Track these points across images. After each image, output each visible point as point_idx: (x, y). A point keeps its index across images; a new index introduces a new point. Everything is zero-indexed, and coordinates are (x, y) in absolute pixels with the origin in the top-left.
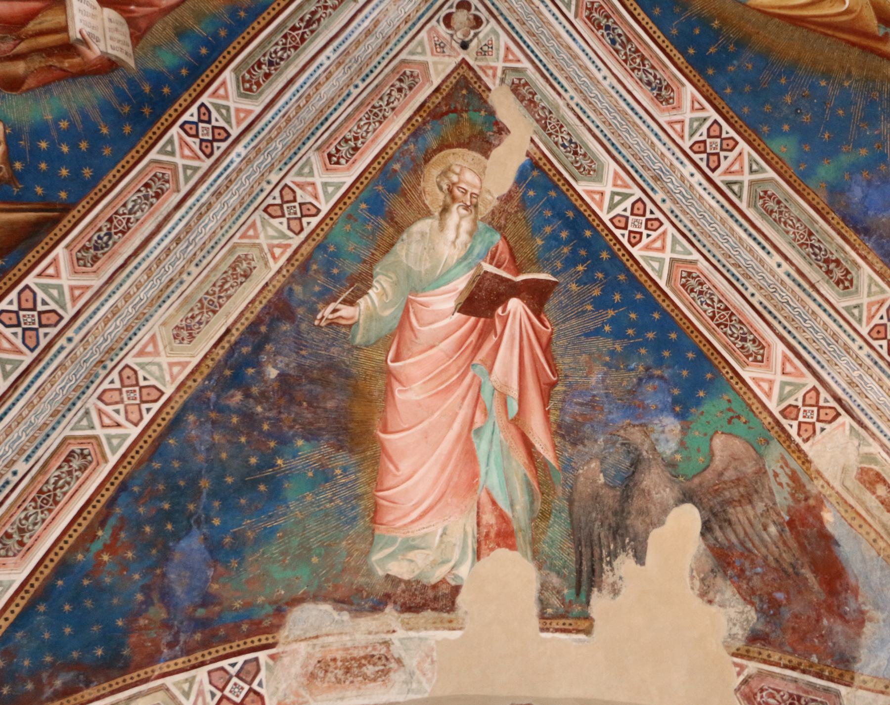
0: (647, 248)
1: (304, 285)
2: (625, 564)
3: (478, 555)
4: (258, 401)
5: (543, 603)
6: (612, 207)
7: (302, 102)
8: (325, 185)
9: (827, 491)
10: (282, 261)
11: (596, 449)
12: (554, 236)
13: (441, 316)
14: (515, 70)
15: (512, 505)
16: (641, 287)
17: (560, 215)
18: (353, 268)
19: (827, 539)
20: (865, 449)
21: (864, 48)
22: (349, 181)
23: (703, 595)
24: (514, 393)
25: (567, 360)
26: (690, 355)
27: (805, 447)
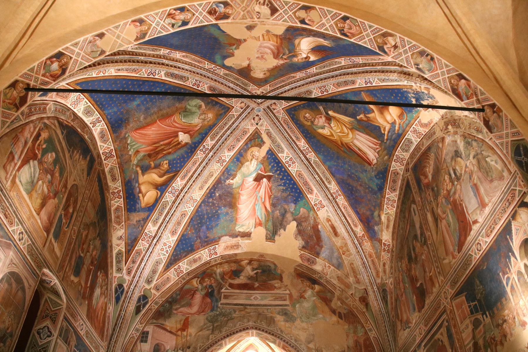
0: (292, 168)
1: (224, 176)
2: (282, 231)
3: (255, 227)
4: (215, 200)
5: (266, 237)
6: (285, 159)
7: (223, 144)
8: (227, 155)
9: (320, 222)
10: (219, 172)
11: (278, 208)
12: (273, 165)
13: (250, 182)
14: (268, 129)
15: (262, 218)
16: (290, 176)
17: (275, 161)
18: (233, 173)
19: (318, 231)
20: (328, 214)
21: (338, 147)
22: (232, 154)
23: (295, 238)
24: (263, 197)
25: (274, 191)
26: (298, 191)
27: (317, 212)
